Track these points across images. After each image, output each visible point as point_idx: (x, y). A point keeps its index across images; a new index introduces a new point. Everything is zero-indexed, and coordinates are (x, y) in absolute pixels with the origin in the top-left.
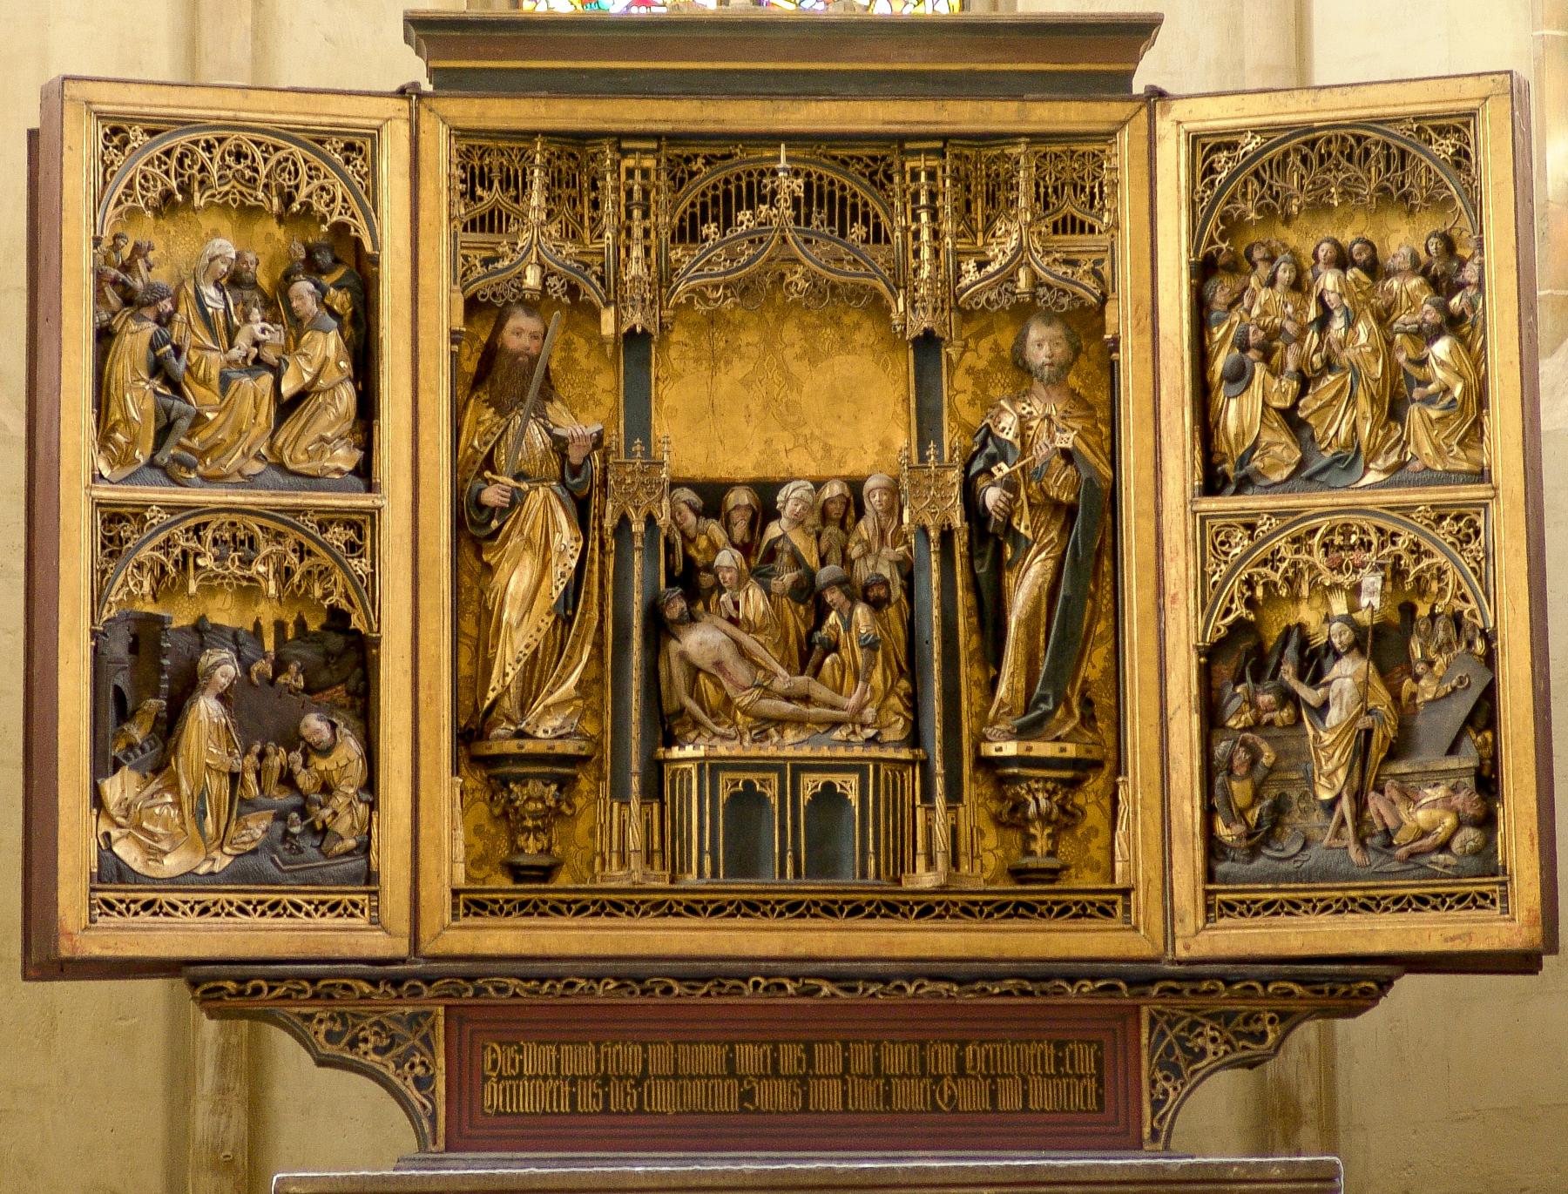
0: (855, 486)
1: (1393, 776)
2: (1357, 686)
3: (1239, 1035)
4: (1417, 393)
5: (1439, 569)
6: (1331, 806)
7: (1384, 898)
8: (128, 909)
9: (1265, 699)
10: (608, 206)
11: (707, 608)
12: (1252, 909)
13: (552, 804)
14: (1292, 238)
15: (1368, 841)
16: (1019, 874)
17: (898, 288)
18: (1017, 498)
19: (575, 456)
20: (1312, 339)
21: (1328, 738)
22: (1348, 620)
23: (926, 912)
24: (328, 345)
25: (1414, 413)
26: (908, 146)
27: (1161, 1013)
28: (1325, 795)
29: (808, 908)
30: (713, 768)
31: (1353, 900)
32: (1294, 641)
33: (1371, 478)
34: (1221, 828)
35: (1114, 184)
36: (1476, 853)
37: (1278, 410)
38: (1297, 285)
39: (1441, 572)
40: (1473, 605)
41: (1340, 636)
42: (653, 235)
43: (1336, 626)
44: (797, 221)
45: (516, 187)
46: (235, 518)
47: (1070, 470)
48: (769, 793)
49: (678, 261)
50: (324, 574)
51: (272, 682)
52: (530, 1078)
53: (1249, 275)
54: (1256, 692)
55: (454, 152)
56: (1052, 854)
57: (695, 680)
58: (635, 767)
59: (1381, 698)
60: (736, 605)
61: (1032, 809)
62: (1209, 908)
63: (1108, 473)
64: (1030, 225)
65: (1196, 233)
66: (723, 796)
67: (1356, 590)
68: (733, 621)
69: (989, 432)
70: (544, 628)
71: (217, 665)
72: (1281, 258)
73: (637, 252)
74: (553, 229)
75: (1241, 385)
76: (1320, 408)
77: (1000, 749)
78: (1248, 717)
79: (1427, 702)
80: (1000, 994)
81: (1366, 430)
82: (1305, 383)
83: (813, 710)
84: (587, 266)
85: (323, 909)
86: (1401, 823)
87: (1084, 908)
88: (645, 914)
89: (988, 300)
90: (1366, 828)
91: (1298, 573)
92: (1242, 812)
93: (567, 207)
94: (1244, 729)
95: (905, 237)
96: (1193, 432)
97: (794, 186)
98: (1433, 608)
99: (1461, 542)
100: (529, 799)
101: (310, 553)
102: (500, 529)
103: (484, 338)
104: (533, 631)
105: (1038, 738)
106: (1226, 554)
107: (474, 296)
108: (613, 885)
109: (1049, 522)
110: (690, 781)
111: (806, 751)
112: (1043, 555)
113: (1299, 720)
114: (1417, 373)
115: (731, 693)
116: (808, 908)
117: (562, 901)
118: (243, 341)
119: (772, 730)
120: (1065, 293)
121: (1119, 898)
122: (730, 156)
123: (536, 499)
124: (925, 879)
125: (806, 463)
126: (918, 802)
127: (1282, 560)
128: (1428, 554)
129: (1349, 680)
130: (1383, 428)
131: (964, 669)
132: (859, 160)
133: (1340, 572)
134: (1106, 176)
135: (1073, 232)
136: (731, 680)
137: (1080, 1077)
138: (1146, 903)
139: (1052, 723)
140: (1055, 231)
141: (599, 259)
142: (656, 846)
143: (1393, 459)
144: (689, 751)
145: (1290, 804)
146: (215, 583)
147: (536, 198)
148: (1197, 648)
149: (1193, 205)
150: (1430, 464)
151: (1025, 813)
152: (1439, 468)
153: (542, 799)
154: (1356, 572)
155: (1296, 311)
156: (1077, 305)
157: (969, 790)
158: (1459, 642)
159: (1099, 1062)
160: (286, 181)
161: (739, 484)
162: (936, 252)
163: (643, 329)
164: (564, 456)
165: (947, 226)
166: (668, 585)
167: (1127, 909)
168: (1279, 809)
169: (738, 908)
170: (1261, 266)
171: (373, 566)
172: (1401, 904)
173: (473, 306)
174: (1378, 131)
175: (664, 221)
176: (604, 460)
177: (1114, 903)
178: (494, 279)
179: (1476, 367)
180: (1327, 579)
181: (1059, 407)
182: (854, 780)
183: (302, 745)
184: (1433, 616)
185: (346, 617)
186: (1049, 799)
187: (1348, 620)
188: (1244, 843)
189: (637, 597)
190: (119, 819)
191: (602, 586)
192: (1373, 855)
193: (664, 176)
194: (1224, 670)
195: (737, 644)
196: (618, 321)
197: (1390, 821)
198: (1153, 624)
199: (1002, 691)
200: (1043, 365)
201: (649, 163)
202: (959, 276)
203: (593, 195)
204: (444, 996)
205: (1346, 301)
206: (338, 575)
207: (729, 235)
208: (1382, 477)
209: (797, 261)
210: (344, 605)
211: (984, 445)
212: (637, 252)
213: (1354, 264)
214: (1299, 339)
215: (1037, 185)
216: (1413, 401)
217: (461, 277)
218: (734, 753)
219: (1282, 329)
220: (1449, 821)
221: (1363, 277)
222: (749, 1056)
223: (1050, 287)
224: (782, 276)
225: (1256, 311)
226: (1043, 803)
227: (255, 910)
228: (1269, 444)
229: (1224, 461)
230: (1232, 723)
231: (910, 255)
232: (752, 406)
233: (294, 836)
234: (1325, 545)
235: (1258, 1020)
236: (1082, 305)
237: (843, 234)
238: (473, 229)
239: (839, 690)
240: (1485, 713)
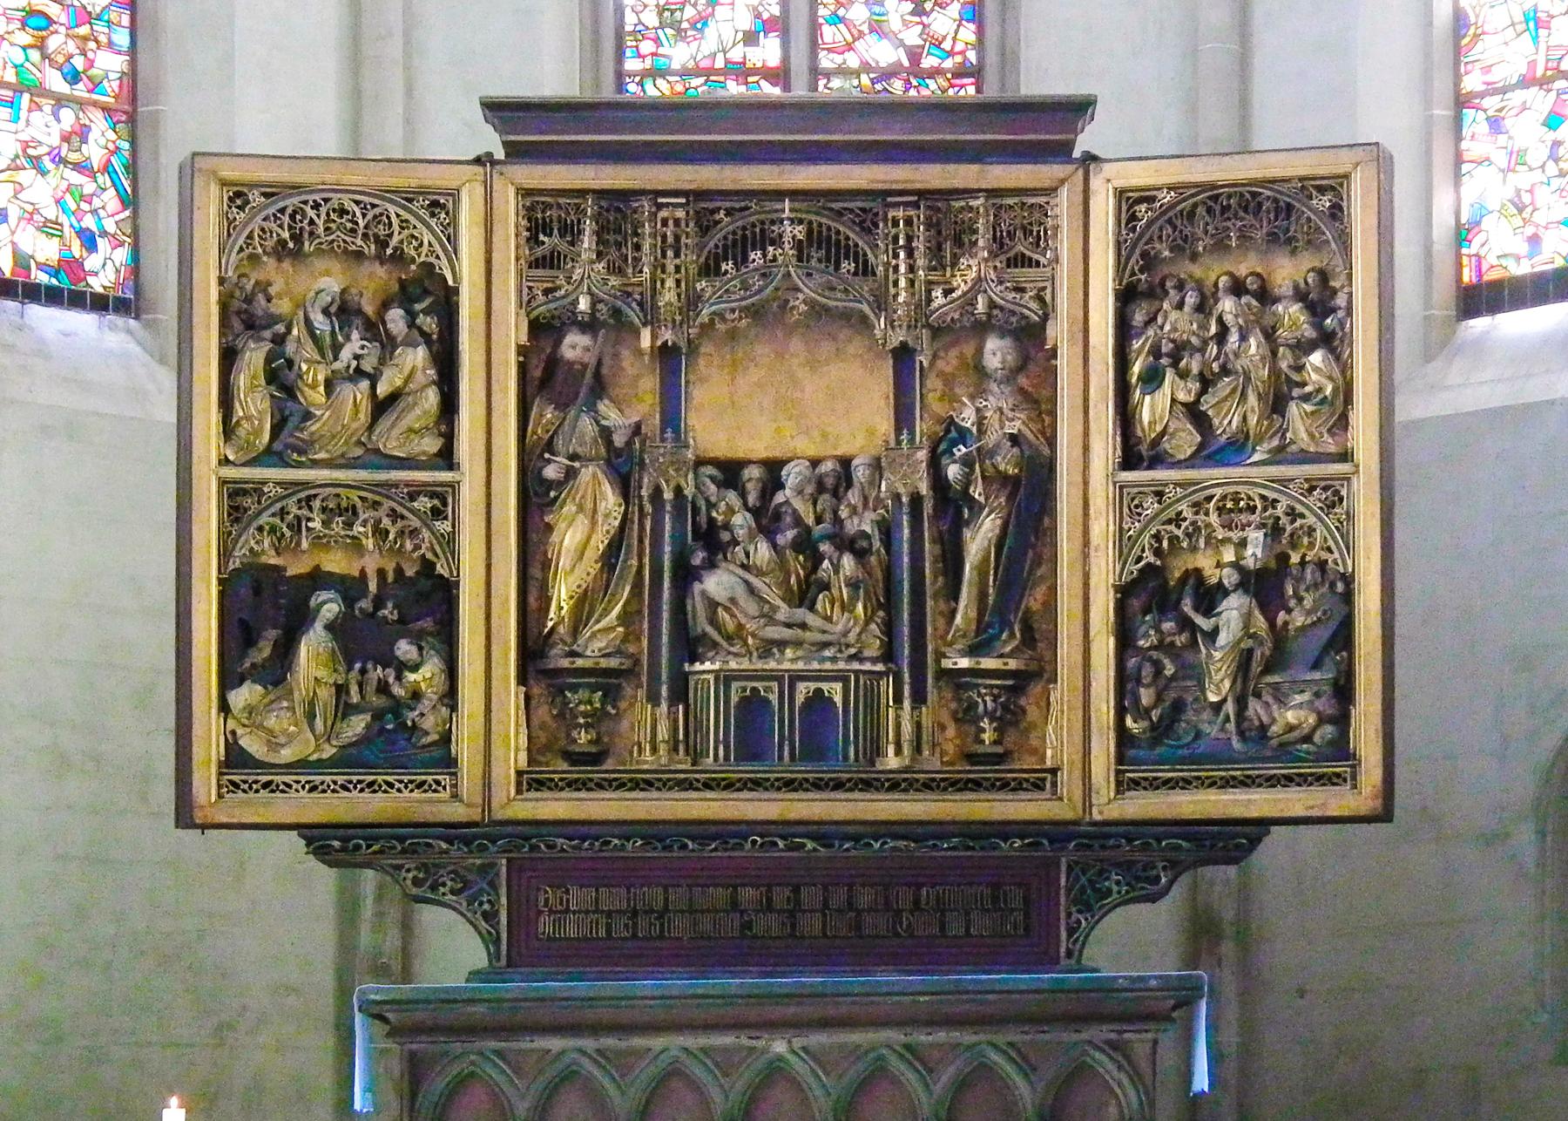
0: (845, 462)
1: (1268, 684)
2: (1241, 615)
3: (1138, 879)
4: (1296, 392)
5: (1310, 527)
6: (1218, 707)
7: (1258, 776)
9: (1168, 626)
10: (646, 247)
11: (725, 558)
12: (1154, 785)
13: (598, 705)
14: (1197, 271)
15: (1247, 734)
16: (972, 758)
17: (880, 310)
18: (972, 470)
19: (619, 440)
20: (1213, 349)
21: (1217, 655)
22: (1236, 565)
23: (894, 786)
24: (417, 357)
25: (1293, 409)
26: (889, 199)
27: (1077, 863)
28: (1213, 698)
29: (801, 784)
30: (725, 679)
31: (1234, 778)
32: (1191, 581)
33: (1256, 457)
34: (1129, 722)
35: (1056, 228)
36: (1331, 743)
37: (1183, 404)
38: (1202, 308)
39: (1311, 530)
40: (1337, 555)
41: (1230, 577)
42: (683, 271)
43: (1226, 571)
44: (800, 259)
45: (573, 234)
46: (338, 490)
47: (1015, 450)
48: (771, 697)
49: (703, 290)
50: (414, 533)
51: (373, 615)
52: (574, 912)
53: (1162, 300)
54: (1160, 621)
55: (520, 207)
56: (995, 743)
57: (715, 612)
58: (664, 677)
59: (1260, 622)
60: (747, 555)
61: (981, 708)
62: (1119, 783)
63: (1046, 451)
64: (986, 260)
65: (1120, 267)
66: (734, 699)
67: (1243, 544)
68: (743, 566)
69: (951, 421)
70: (593, 572)
71: (324, 603)
72: (1188, 287)
73: (670, 283)
74: (600, 266)
75: (1154, 385)
76: (1218, 403)
77: (956, 663)
78: (1153, 639)
79: (1297, 629)
80: (949, 849)
81: (1253, 420)
82: (1206, 382)
83: (808, 633)
84: (629, 294)
86: (1274, 721)
87: (1020, 783)
88: (670, 789)
89: (952, 319)
90: (1246, 724)
91: (1197, 529)
92: (1148, 711)
93: (613, 249)
94: (1149, 649)
95: (887, 270)
96: (1114, 423)
97: (796, 232)
98: (1304, 556)
99: (1328, 507)
100: (580, 702)
101: (403, 517)
102: (556, 498)
103: (548, 351)
104: (584, 576)
105: (987, 655)
106: (1140, 514)
107: (537, 317)
108: (645, 767)
109: (999, 490)
110: (709, 688)
111: (800, 665)
112: (993, 516)
113: (1193, 644)
114: (1296, 377)
115: (743, 621)
116: (801, 784)
117: (605, 779)
118: (346, 354)
119: (775, 650)
120: (1013, 313)
121: (1049, 776)
122: (747, 208)
123: (587, 473)
124: (891, 761)
125: (808, 447)
126: (891, 703)
127: (1185, 519)
128: (1302, 516)
129: (1235, 613)
130: (1268, 418)
131: (930, 603)
132: (851, 211)
133: (1231, 529)
134: (1050, 222)
135: (1023, 267)
136: (741, 612)
137: (1013, 910)
138: (1069, 781)
139: (998, 644)
140: (1008, 266)
141: (639, 289)
142: (681, 737)
143: (1275, 442)
144: (708, 666)
145: (1186, 705)
147: (587, 242)
148: (1113, 586)
149: (1118, 245)
151: (976, 712)
153: (590, 702)
154: (1243, 530)
155: (1199, 327)
156: (1023, 323)
157: (932, 694)
158: (1323, 585)
159: (1026, 900)
160: (382, 231)
161: (754, 463)
162: (912, 283)
163: (674, 343)
164: (609, 442)
165: (921, 262)
166: (693, 540)
167: (1054, 784)
168: (1178, 707)
169: (745, 784)
170: (1172, 292)
171: (454, 527)
172: (1272, 782)
173: (536, 327)
174: (1271, 189)
175: (690, 259)
176: (643, 443)
177: (1044, 780)
178: (553, 306)
179: (1343, 372)
180: (1220, 534)
181: (1010, 401)
182: (838, 686)
183: (395, 662)
184: (1303, 563)
185: (433, 565)
186: (994, 701)
187: (1236, 565)
188: (1148, 734)
189: (667, 549)
191: (641, 541)
192: (1250, 745)
193: (692, 224)
194: (1135, 604)
195: (746, 582)
196: (654, 337)
197: (1265, 719)
198: (1079, 566)
199: (958, 619)
200: (996, 369)
201: (680, 214)
202: (929, 300)
203: (635, 240)
204: (505, 852)
205: (1241, 321)
206: (426, 534)
207: (744, 270)
209: (798, 290)
210: (429, 556)
211: (948, 431)
212: (670, 283)
213: (1247, 292)
214: (1202, 350)
215: (995, 232)
216: (1292, 398)
217: (526, 303)
218: (742, 667)
219: (1189, 342)
220: (1312, 720)
221: (1254, 303)
222: (748, 894)
223: (1002, 309)
224: (787, 301)
225: (1167, 327)
226: (990, 705)
228: (1176, 430)
229: (1138, 444)
230: (1141, 643)
231: (891, 285)
232: (765, 405)
234: (1218, 509)
235: (1154, 867)
236: (1028, 324)
237: (837, 268)
238: (537, 267)
239: (828, 619)
240: (1344, 637)
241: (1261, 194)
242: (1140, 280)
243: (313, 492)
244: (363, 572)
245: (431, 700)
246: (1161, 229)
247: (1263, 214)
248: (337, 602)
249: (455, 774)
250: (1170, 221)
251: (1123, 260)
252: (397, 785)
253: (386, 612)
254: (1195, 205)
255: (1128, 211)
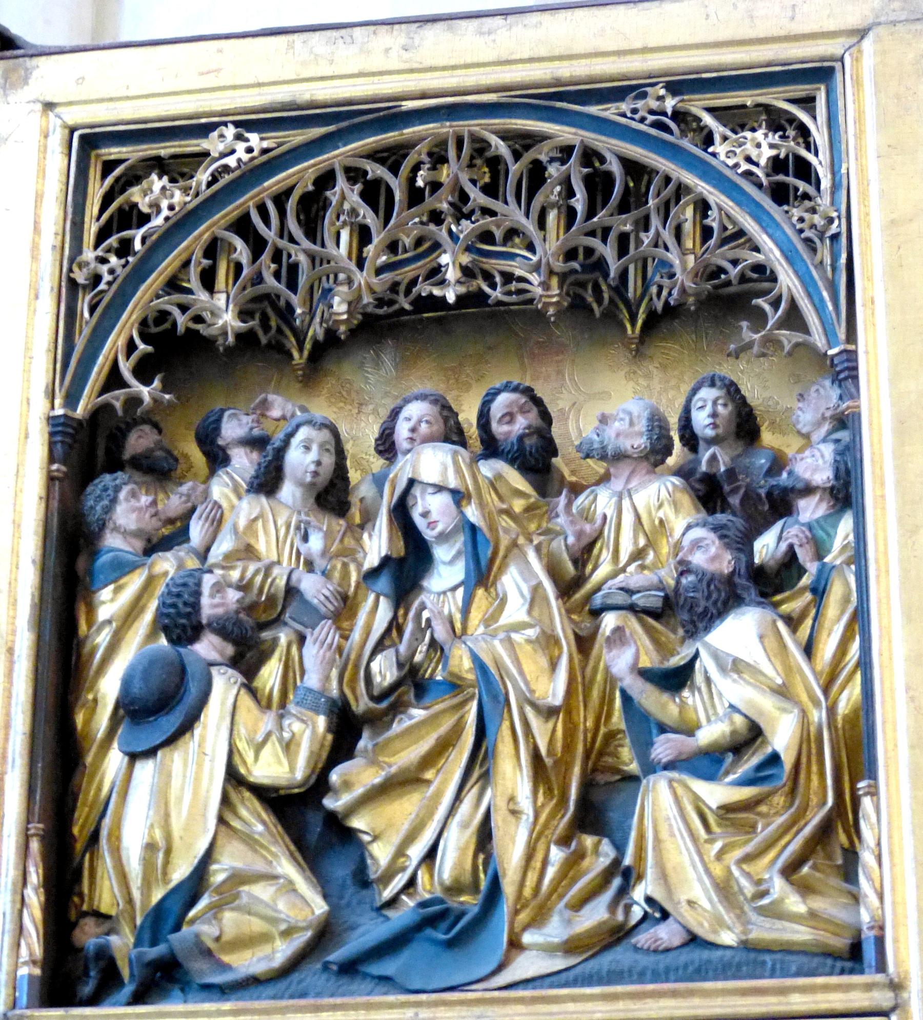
130: (564, 841)
150: (704, 931)
152: (728, 938)
208: (559, 963)
219: (291, 591)
221: (515, 479)
225: (224, 545)
228: (239, 879)
241: (541, 138)
242: (134, 401)
246: (212, 250)
247: (552, 192)
250: (242, 226)
251: (80, 343)
254: (326, 180)
255: (107, 200)
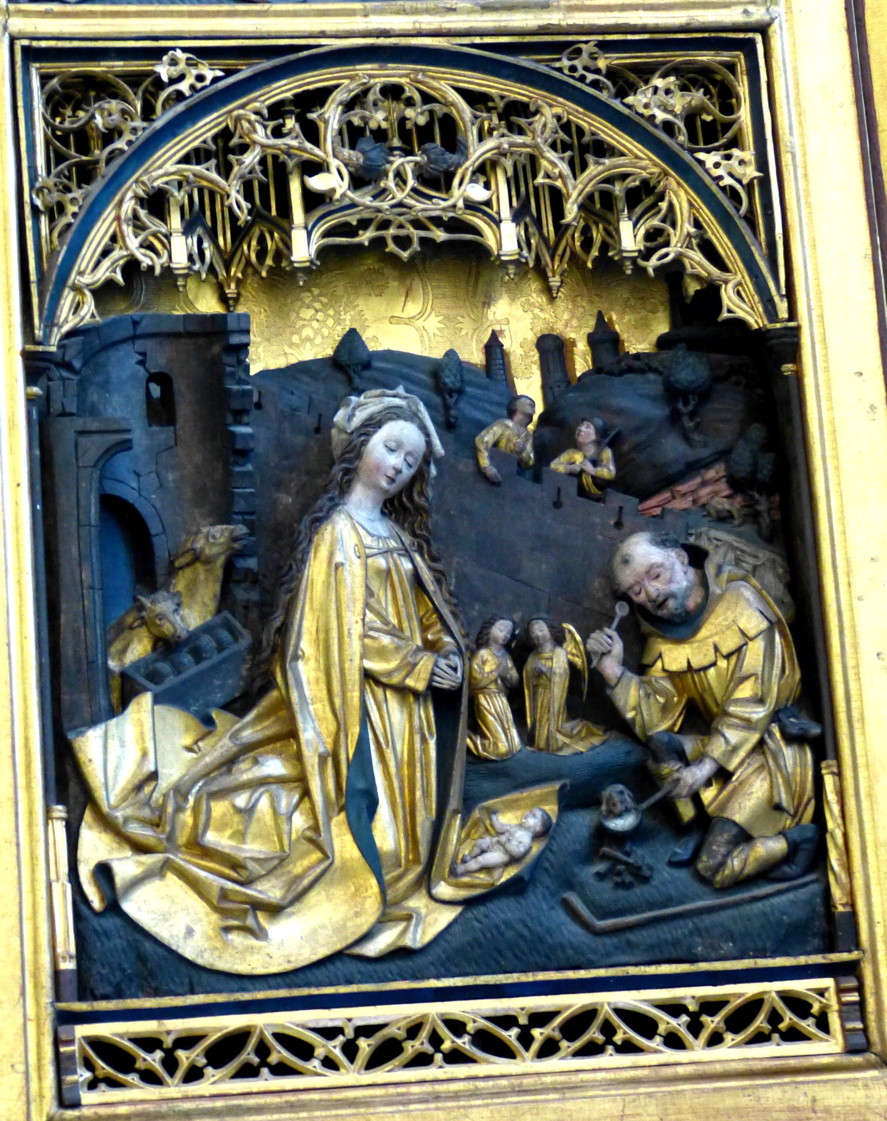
8: (171, 1064)
85: (712, 1023)
101: (602, 149)
146: (365, 237)
171: (762, 165)
183: (621, 610)
185: (711, 292)
190: (136, 830)
227: (526, 1040)
233: (619, 838)
243: (313, 80)
244: (493, 347)
245: (748, 724)
248: (413, 417)
249: (852, 969)
252: (666, 1022)
253: (578, 457)
